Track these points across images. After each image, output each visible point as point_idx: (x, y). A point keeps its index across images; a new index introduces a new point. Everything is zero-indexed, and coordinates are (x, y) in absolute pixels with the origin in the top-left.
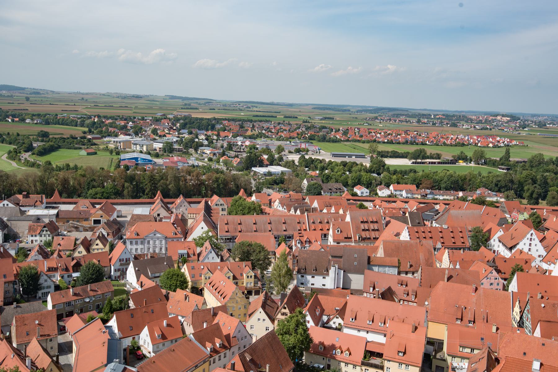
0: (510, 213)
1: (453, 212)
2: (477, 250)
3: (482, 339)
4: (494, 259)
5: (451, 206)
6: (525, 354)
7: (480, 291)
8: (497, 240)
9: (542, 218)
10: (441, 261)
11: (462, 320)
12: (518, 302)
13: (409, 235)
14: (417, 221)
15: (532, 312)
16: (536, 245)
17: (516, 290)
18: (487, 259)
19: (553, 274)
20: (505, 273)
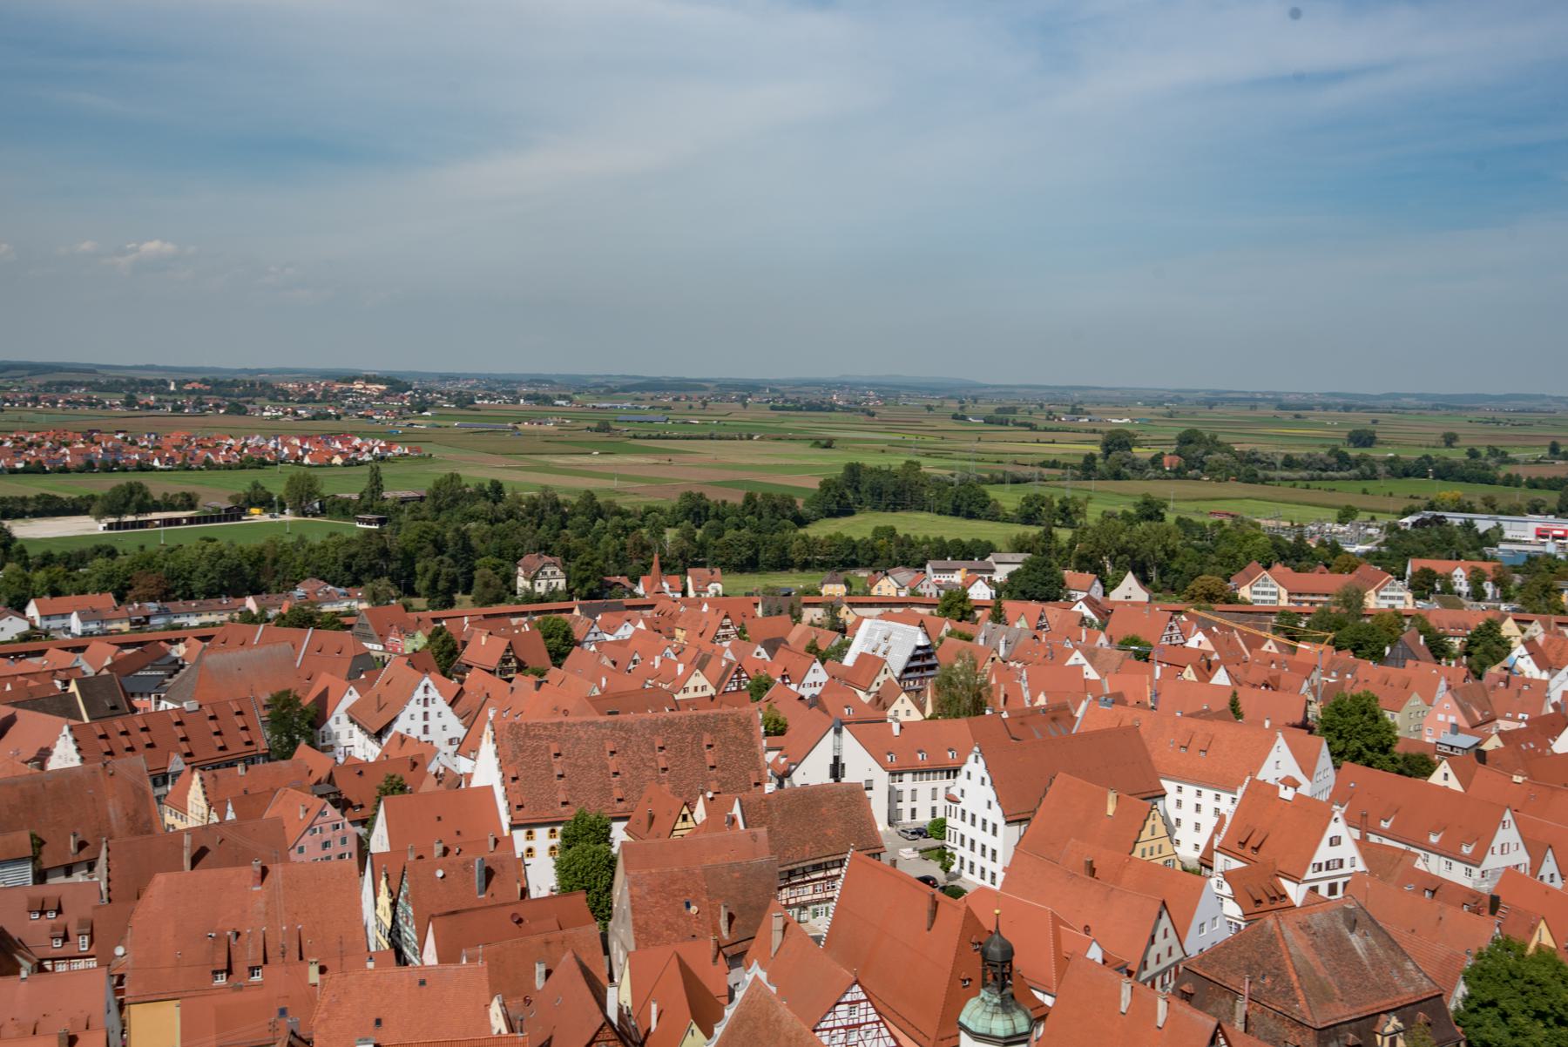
0: (382, 638)
1: (214, 659)
2: (287, 756)
3: (283, 1012)
4: (331, 775)
5: (217, 642)
6: (378, 1022)
7: (276, 871)
8: (344, 718)
9: (458, 640)
10: (182, 809)
11: (229, 972)
12: (383, 882)
13: (79, 750)
14: (109, 699)
15: (414, 899)
16: (439, 714)
17: (385, 848)
18: (315, 778)
19: (475, 783)
20: (361, 806)
